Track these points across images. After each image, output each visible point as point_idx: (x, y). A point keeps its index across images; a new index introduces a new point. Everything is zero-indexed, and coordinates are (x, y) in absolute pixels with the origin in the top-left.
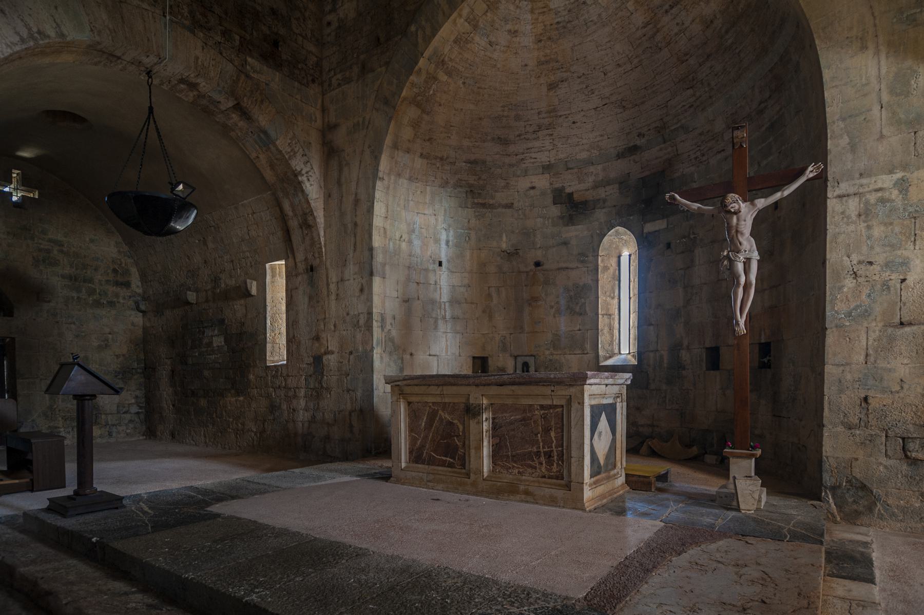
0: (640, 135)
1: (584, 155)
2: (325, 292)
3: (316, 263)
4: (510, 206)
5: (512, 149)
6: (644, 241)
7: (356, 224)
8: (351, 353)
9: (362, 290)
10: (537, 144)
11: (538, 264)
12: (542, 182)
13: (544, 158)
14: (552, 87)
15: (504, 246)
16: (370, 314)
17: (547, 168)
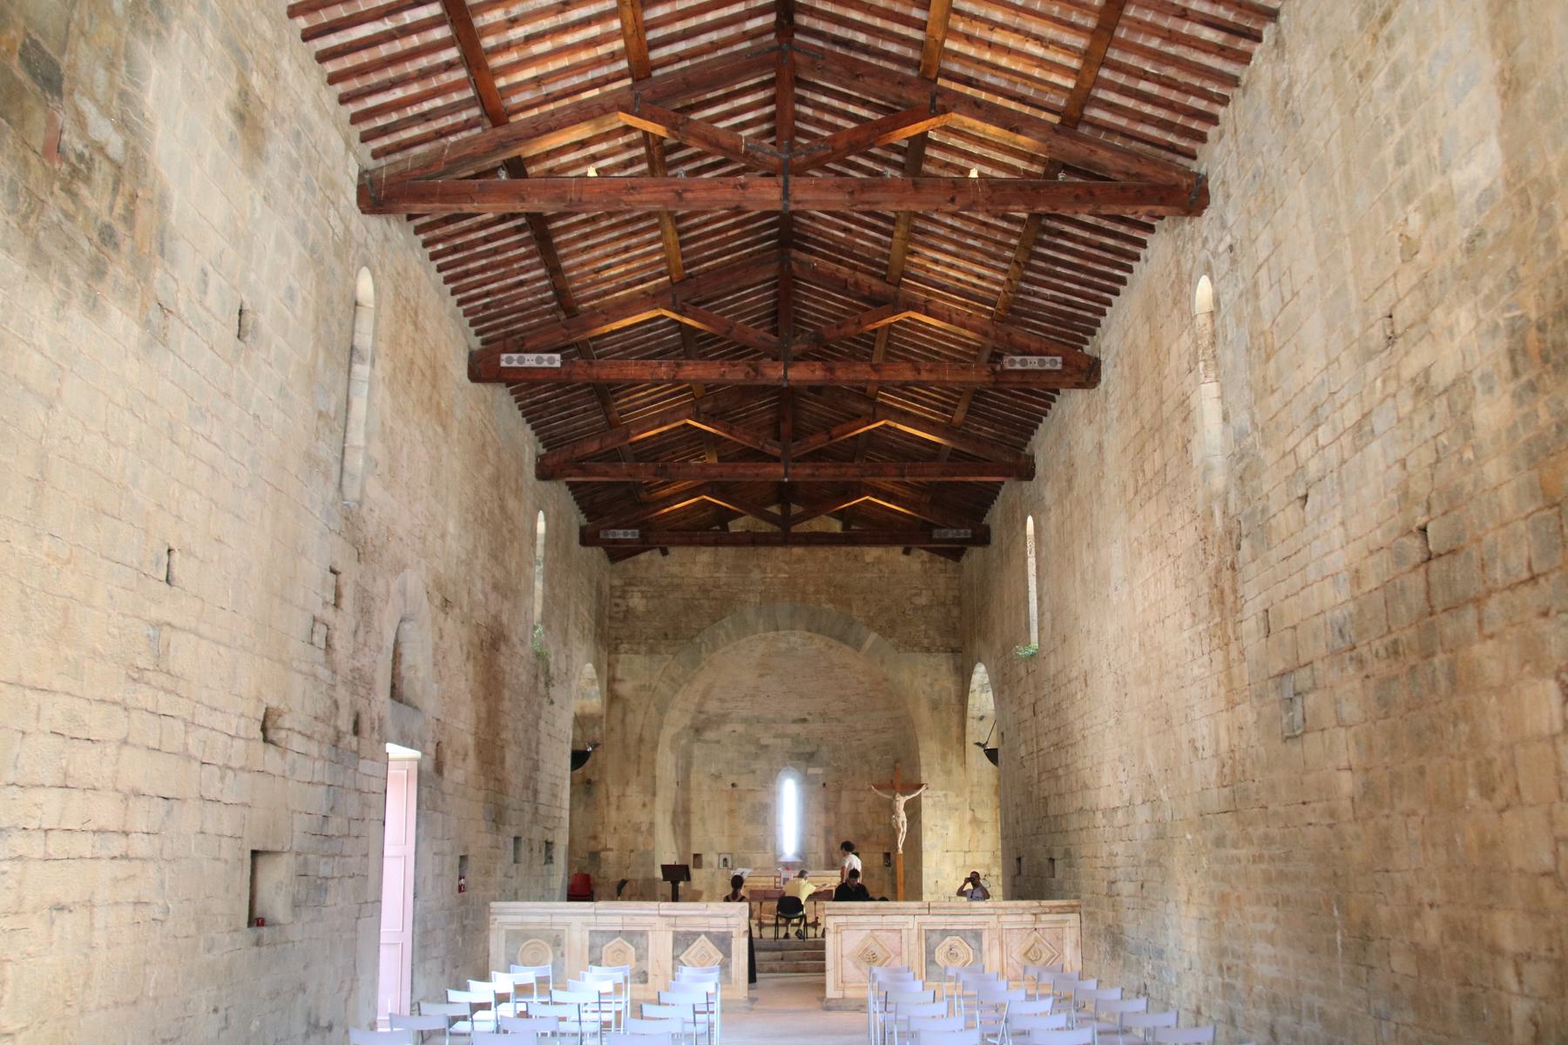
0: (809, 714)
1: (770, 716)
2: (604, 802)
3: (595, 778)
4: (718, 742)
5: (726, 705)
6: (806, 781)
7: (639, 757)
8: (632, 851)
9: (644, 805)
10: (742, 704)
11: (733, 785)
12: (740, 728)
13: (744, 713)
14: (761, 676)
15: (713, 771)
16: (652, 824)
17: (745, 720)
